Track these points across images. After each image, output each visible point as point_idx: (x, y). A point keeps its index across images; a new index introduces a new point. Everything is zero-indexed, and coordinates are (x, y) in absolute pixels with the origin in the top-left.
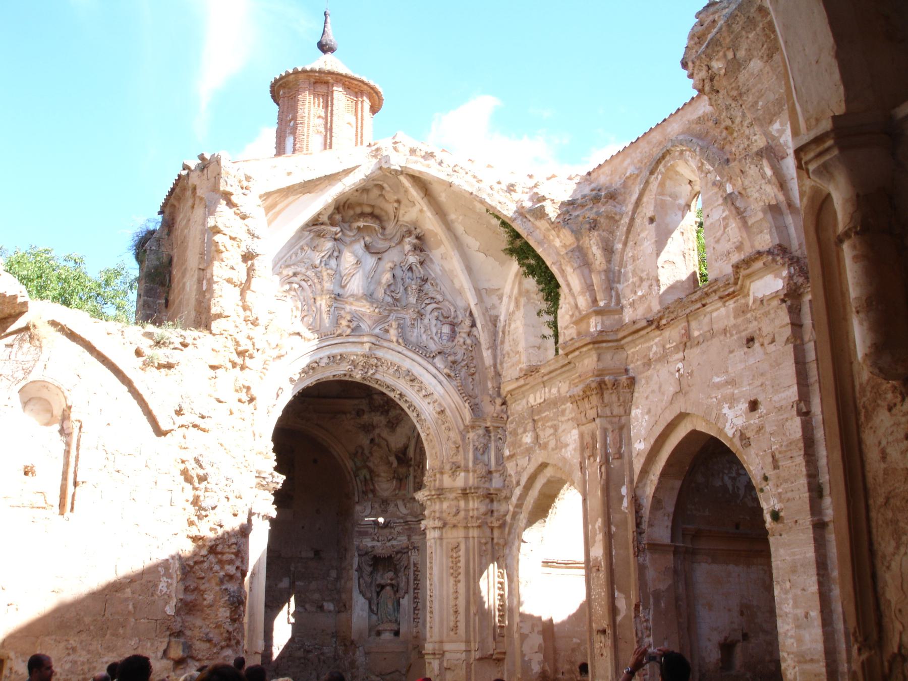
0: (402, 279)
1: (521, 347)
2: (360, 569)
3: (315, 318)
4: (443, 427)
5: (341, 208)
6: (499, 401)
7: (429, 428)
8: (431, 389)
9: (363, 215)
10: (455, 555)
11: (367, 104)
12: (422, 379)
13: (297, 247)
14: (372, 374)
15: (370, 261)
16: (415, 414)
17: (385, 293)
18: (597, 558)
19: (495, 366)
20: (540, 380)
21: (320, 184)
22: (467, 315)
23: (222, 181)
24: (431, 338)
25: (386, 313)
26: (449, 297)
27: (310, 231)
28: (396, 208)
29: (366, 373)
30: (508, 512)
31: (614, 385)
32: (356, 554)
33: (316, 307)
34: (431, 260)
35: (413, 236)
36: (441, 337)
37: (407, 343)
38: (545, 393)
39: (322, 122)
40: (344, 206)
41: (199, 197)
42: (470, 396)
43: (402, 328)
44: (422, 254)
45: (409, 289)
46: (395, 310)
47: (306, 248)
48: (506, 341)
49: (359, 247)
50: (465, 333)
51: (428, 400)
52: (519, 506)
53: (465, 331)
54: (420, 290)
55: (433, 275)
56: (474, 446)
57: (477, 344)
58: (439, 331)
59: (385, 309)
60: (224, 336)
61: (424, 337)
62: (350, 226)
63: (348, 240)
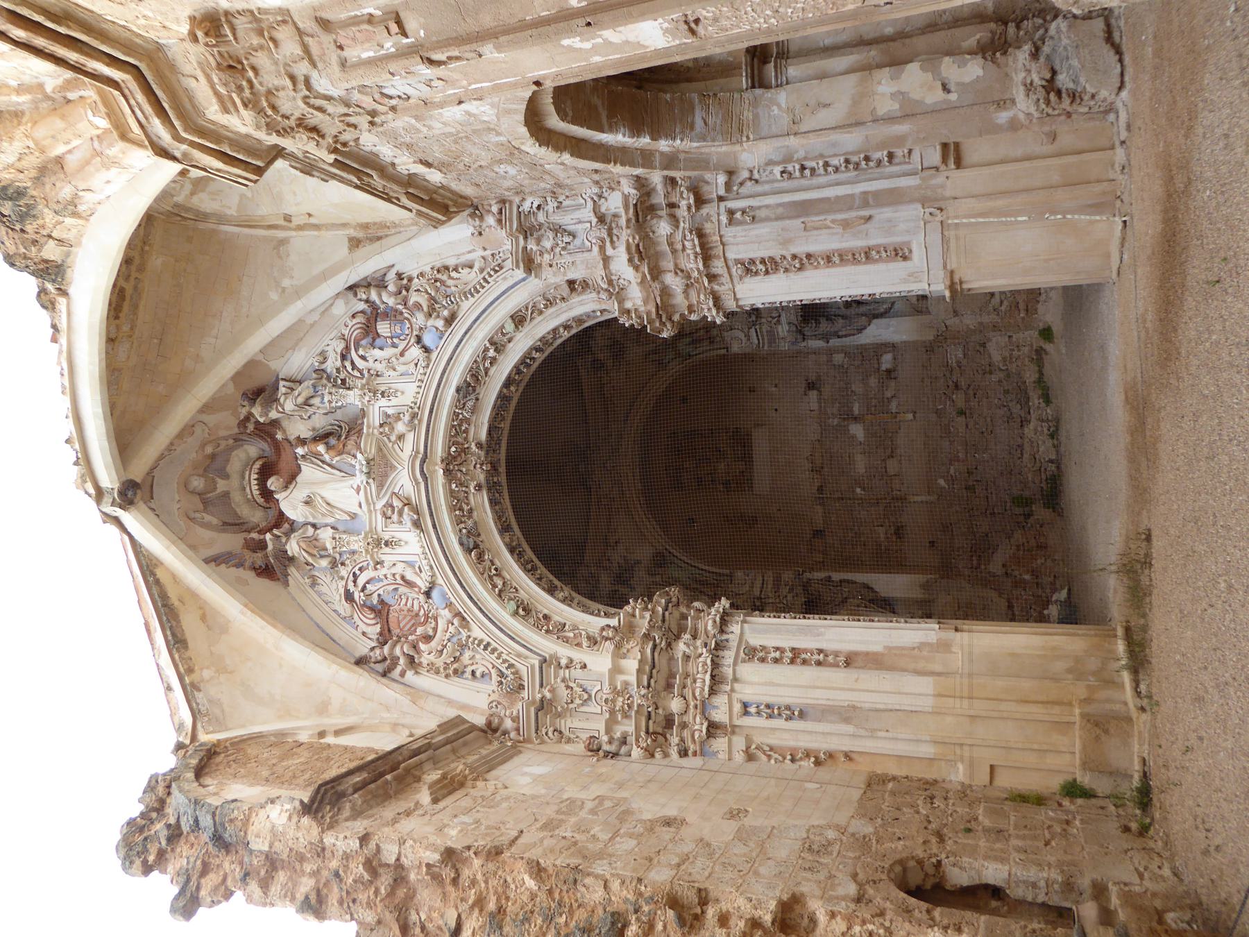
2: (826, 337)
10: (761, 267)
16: (537, 355)
18: (666, 31)
24: (402, 354)
30: (666, 178)
31: (231, 67)
32: (804, 344)
52: (646, 158)
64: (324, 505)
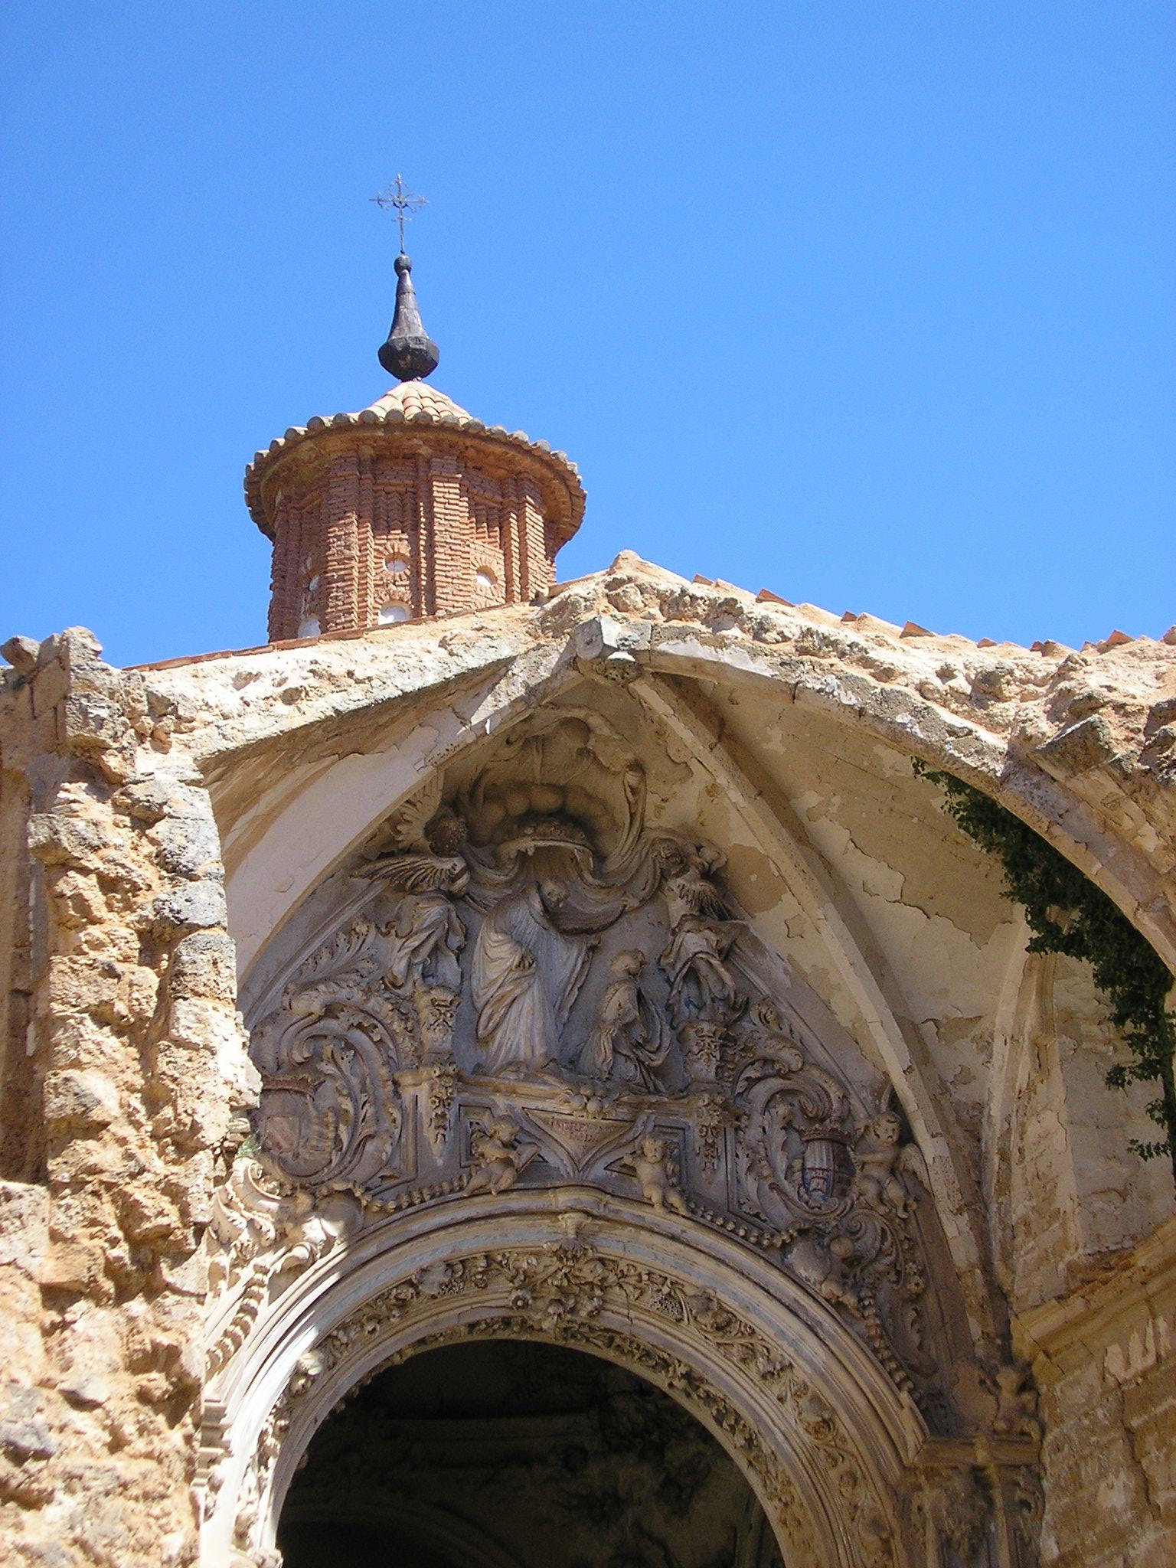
0: (669, 1007)
1: (1064, 1200)
3: (398, 1145)
4: (834, 1474)
5: (466, 799)
6: (1008, 1379)
7: (789, 1482)
8: (784, 1351)
9: (532, 817)
11: (535, 521)
12: (753, 1319)
13: (334, 927)
14: (591, 1315)
15: (565, 957)
16: (740, 1441)
17: (615, 1051)
19: (986, 1266)
20: (1136, 1295)
21: (393, 720)
22: (884, 1107)
23: (71, 708)
25: (623, 1112)
26: (819, 1053)
27: (371, 875)
28: (634, 791)
29: (573, 1310)
33: (401, 1108)
34: (756, 944)
35: (693, 872)
36: (804, 1183)
37: (696, 1206)
38: (1157, 1336)
39: (402, 570)
40: (472, 794)
41: (9, 772)
42: (911, 1367)
43: (677, 1160)
44: (725, 927)
45: (691, 1032)
46: (651, 1105)
47: (362, 928)
48: (1016, 1180)
49: (527, 915)
50: (880, 1164)
51: (777, 1389)
53: (879, 1157)
54: (727, 1040)
55: (765, 989)
56: (940, 1531)
57: (920, 1195)
58: (797, 1164)
59: (618, 1103)
60: (89, 1188)
61: (751, 1185)
62: (495, 855)
63: (491, 895)
64: (517, 992)
